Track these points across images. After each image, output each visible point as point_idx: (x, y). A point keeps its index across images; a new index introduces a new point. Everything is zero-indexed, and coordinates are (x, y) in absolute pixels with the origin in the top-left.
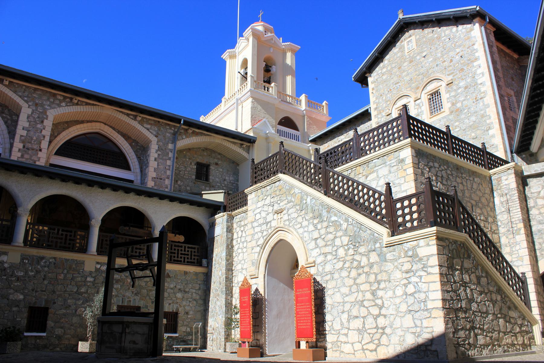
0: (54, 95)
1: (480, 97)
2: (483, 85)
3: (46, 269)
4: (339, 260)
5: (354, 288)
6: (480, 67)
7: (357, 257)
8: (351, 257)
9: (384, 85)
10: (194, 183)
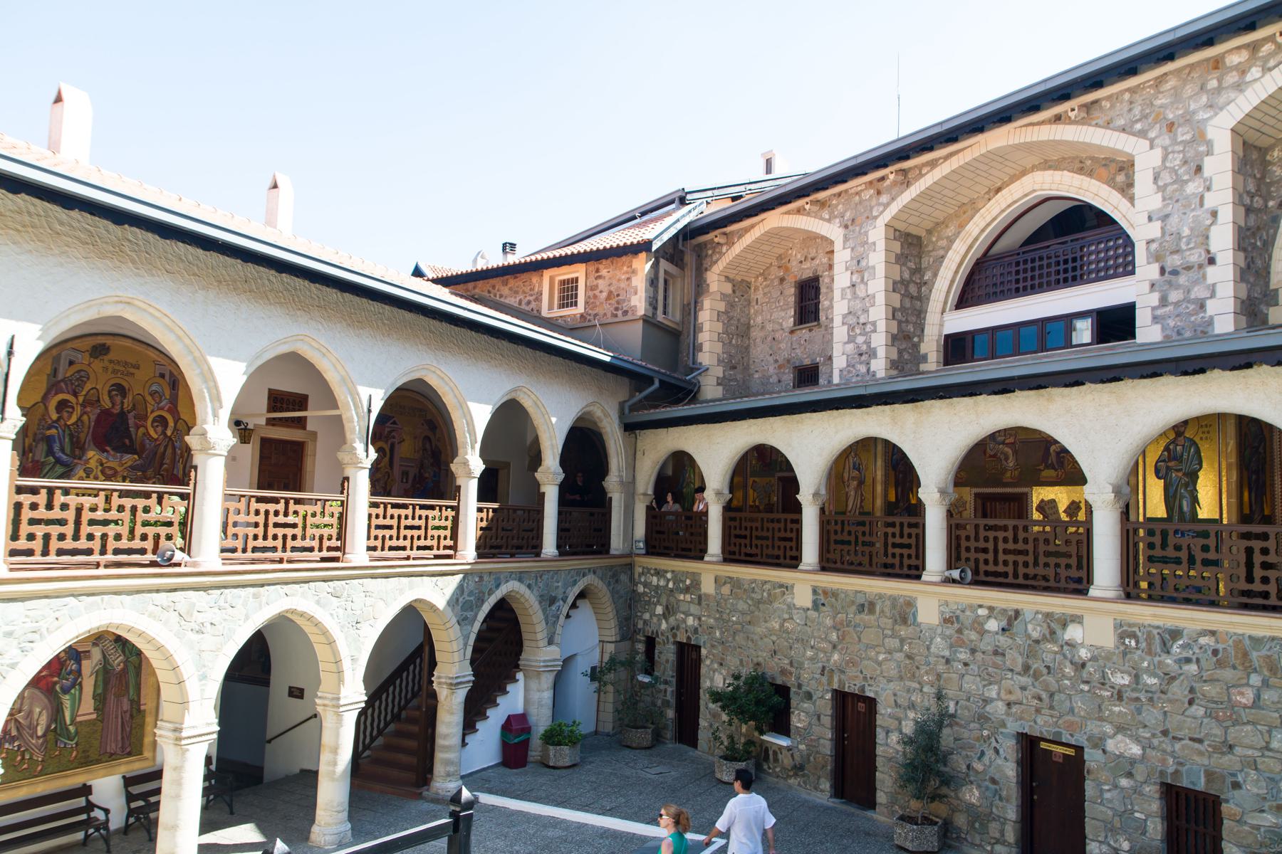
0: (1217, 63)
3: (1193, 668)
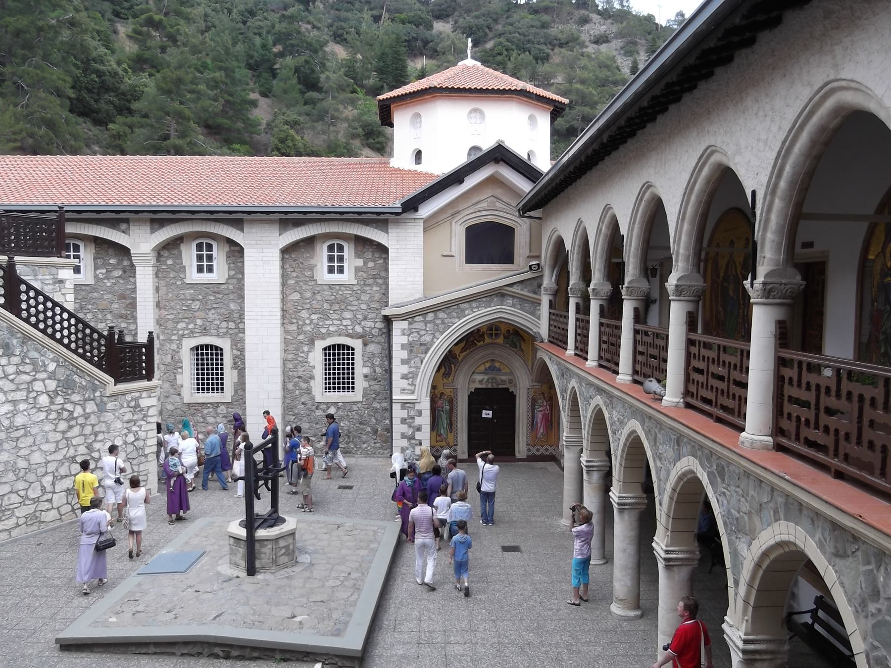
4: (39, 410)
7: (69, 407)
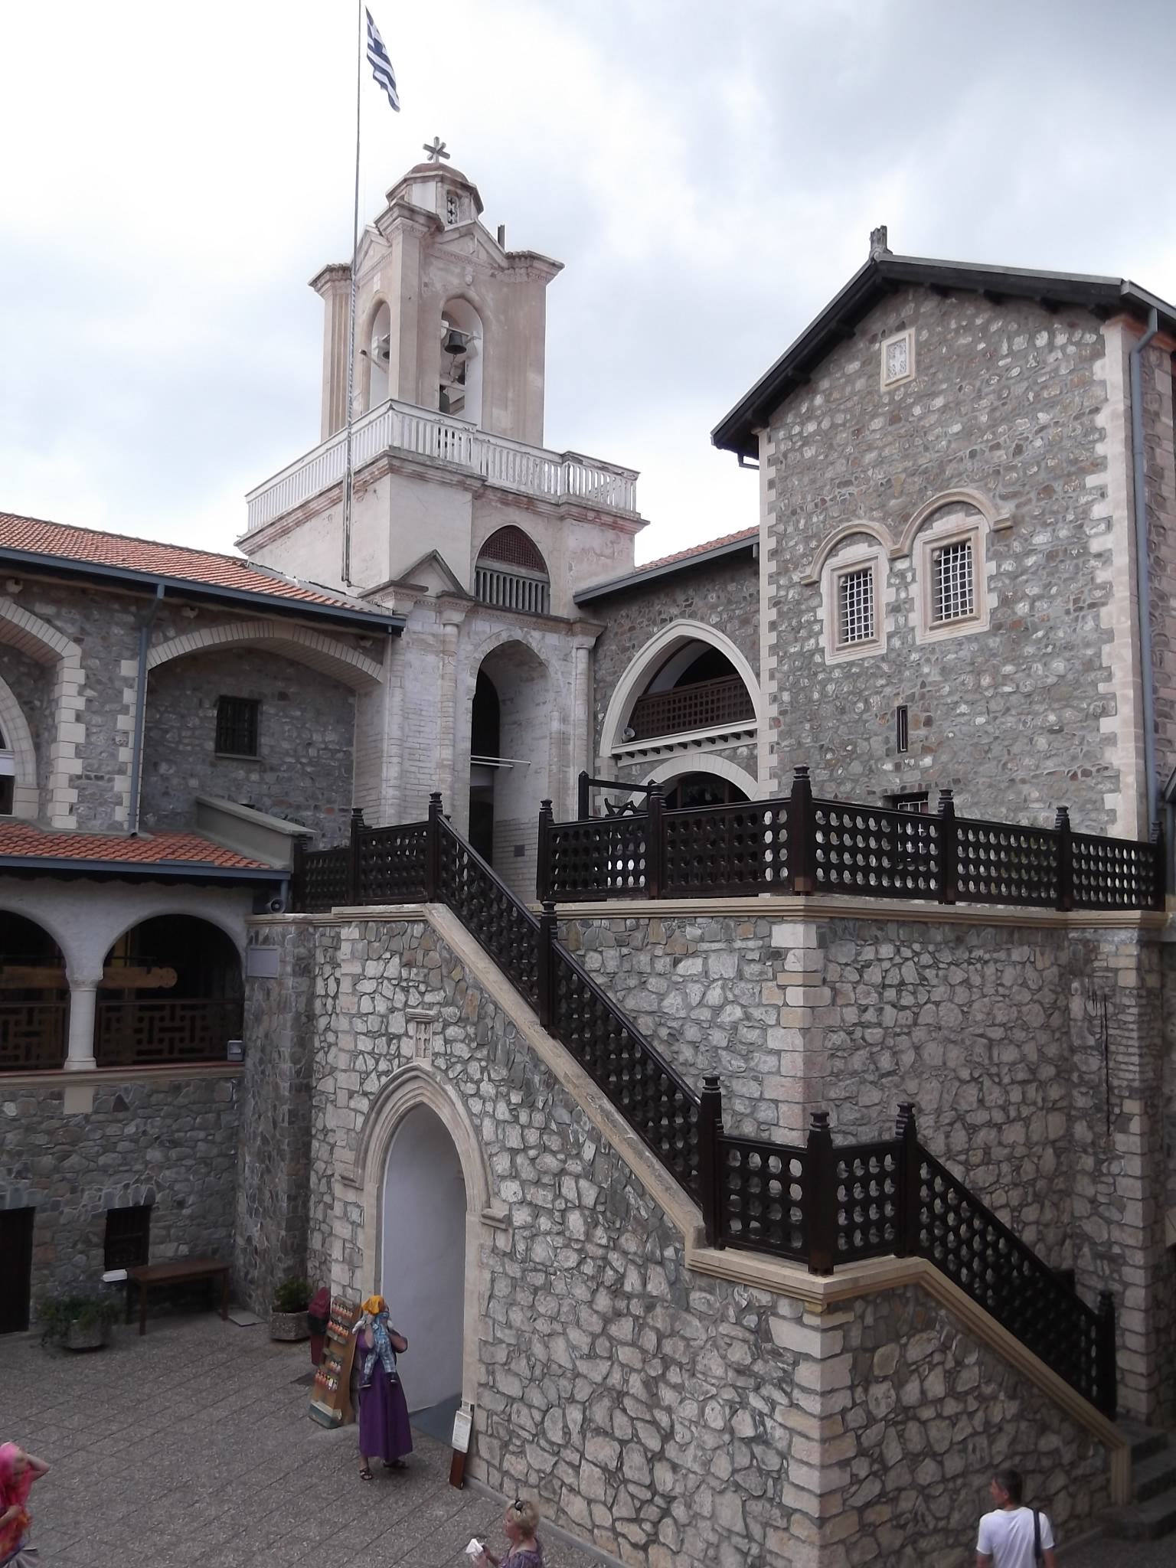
1: (1089, 601)
2: (1104, 563)
5: (602, 1346)
6: (1103, 495)
8: (600, 1252)
9: (806, 480)
10: (213, 765)
